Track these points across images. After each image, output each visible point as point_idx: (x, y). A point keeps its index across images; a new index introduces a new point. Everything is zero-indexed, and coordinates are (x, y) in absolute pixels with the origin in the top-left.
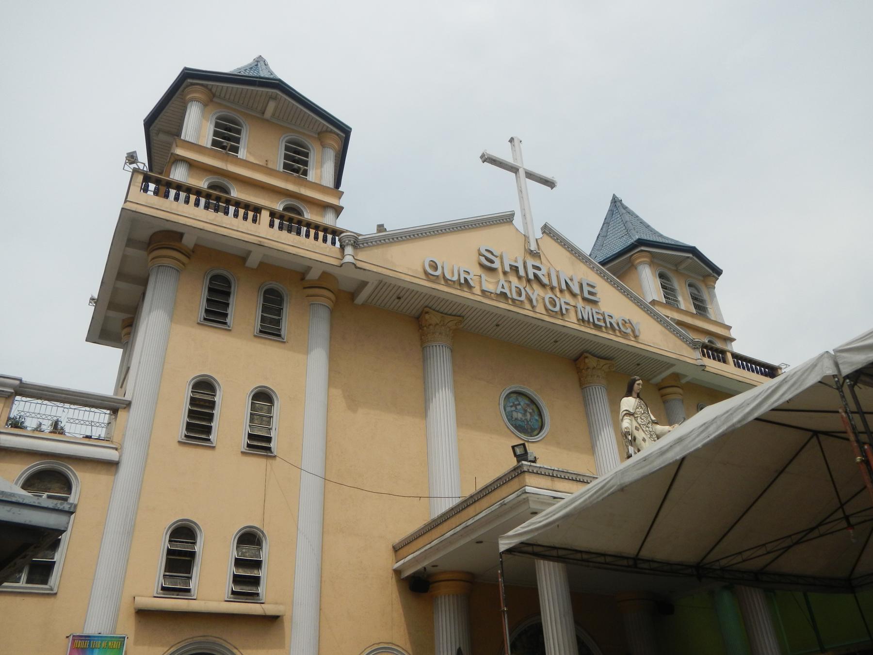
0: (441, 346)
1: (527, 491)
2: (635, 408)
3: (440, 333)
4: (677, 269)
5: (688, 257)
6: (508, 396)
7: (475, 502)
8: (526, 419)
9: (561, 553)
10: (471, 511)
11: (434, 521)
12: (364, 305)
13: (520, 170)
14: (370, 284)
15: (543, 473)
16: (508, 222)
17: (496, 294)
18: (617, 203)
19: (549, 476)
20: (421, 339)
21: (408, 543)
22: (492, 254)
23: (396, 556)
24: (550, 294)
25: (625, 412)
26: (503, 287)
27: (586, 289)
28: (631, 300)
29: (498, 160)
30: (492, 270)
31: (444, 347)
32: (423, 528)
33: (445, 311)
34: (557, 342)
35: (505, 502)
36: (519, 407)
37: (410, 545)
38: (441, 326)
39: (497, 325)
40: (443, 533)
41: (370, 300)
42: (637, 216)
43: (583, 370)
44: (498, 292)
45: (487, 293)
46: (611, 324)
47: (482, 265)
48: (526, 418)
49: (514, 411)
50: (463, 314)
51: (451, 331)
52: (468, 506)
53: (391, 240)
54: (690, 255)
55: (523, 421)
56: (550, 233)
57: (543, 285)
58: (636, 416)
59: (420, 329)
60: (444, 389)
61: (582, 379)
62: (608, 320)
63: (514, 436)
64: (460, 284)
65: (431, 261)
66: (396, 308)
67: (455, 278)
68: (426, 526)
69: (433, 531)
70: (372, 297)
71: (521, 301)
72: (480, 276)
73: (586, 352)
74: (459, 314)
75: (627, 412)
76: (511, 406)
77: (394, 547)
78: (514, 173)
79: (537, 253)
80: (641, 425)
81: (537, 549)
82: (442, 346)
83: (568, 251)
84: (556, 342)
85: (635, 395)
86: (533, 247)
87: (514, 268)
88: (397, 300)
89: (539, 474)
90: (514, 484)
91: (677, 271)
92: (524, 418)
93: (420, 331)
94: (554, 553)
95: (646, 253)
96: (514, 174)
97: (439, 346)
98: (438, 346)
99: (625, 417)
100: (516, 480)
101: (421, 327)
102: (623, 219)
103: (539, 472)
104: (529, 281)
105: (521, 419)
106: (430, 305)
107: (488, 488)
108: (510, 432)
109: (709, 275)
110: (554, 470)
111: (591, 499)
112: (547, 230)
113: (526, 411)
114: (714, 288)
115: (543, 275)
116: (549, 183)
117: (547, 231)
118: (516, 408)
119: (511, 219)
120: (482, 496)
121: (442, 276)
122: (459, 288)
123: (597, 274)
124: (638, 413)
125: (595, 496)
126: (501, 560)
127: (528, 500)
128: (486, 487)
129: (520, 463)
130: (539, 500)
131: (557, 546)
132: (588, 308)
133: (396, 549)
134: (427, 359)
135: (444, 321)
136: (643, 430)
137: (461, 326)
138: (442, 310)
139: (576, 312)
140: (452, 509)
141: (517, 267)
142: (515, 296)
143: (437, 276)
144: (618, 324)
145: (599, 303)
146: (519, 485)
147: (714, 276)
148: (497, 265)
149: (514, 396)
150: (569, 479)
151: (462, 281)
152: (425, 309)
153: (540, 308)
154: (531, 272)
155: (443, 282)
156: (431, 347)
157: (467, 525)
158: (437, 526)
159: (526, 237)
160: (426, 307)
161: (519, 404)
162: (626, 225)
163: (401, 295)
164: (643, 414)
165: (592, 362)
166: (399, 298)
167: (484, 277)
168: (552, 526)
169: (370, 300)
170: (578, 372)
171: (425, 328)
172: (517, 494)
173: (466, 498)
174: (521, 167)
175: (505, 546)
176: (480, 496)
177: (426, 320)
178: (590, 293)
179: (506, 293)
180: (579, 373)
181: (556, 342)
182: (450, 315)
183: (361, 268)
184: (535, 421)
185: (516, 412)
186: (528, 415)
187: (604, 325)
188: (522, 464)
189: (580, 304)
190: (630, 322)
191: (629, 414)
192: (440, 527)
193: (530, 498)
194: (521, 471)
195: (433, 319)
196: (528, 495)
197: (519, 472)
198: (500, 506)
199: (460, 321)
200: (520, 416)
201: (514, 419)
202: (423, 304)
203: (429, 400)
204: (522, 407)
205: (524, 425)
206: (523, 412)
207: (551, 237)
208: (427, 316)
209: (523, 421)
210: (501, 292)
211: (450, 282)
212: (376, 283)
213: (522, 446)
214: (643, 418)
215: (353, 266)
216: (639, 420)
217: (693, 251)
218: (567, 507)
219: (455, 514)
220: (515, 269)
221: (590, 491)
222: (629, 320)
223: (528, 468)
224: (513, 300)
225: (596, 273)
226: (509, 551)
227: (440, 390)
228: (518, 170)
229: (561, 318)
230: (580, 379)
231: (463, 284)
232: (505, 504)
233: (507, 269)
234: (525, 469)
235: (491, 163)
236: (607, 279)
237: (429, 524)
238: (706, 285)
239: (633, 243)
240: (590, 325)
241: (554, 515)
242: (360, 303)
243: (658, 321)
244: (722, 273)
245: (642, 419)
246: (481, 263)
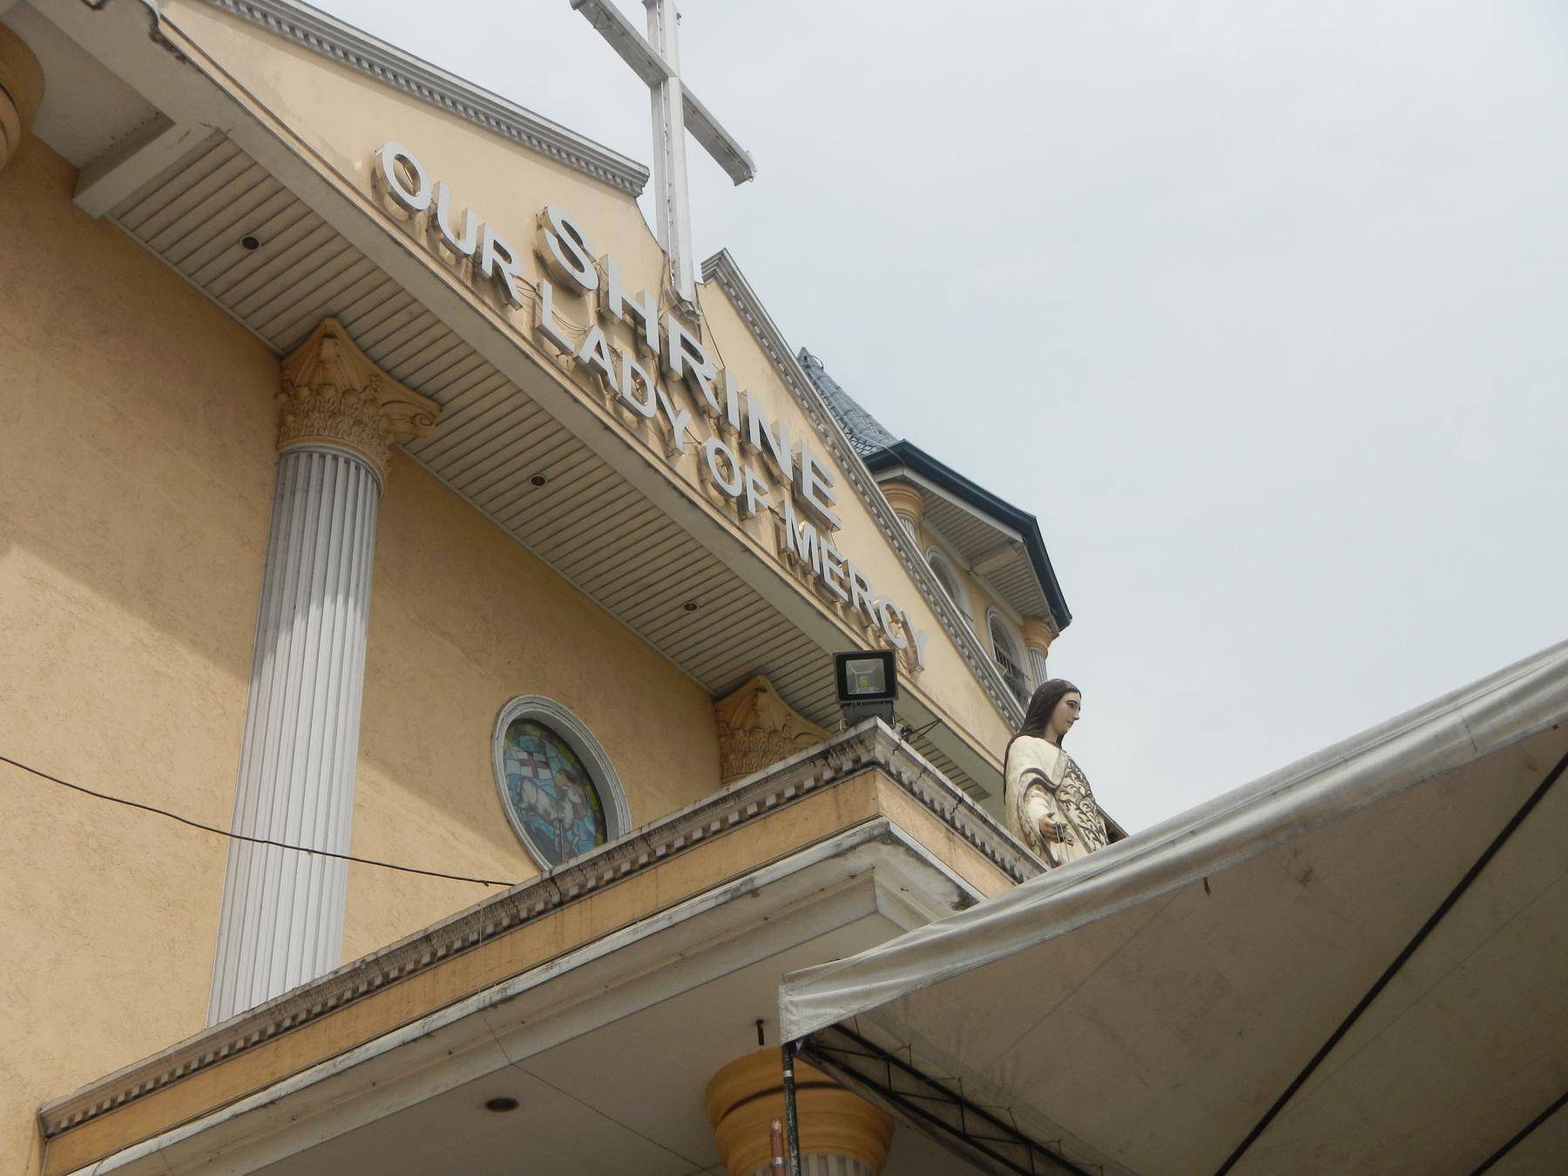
0: (353, 466)
1: (896, 830)
2: (1060, 772)
3: (358, 422)
4: (972, 568)
5: (1012, 542)
6: (519, 726)
7: (561, 904)
8: (561, 821)
9: (973, 1125)
10: (534, 940)
11: (306, 993)
12: (104, 226)
13: (673, 83)
14: (169, 136)
15: (927, 799)
16: (623, 191)
17: (577, 359)
18: (814, 369)
19: (943, 817)
20: (281, 424)
21: (129, 1100)
22: (579, 241)
23: (42, 1156)
24: (713, 442)
25: (1033, 776)
26: (598, 348)
27: (809, 478)
28: (906, 569)
29: (618, 18)
30: (569, 289)
31: (363, 472)
32: (234, 1029)
33: (389, 362)
34: (695, 607)
35: (757, 883)
36: (544, 774)
37: (139, 1105)
38: (365, 402)
39: (538, 481)
40: (345, 1044)
41: (132, 220)
42: (868, 416)
43: (741, 733)
44: (587, 360)
45: (546, 340)
46: (863, 604)
47: (540, 259)
48: (561, 815)
49: (529, 779)
50: (445, 395)
51: (390, 440)
52: (517, 923)
53: (286, 28)
54: (1019, 538)
55: (551, 823)
56: (729, 285)
57: (700, 411)
58: (1064, 797)
59: (284, 390)
60: (340, 599)
61: (732, 757)
62: (856, 588)
63: (526, 858)
64: (476, 273)
65: (401, 158)
66: (218, 286)
67: (467, 247)
68: (255, 1017)
69: (286, 1042)
70: (140, 213)
71: (640, 417)
72: (536, 290)
73: (767, 674)
74: (430, 387)
75: (1038, 776)
76: (523, 763)
77: (42, 1119)
78: (649, 85)
79: (694, 313)
80: (1082, 830)
81: (903, 1083)
82: (358, 468)
83: (768, 358)
84: (690, 607)
85: (1050, 730)
86: (686, 293)
87: (628, 319)
88: (238, 251)
89: (914, 794)
90: (818, 812)
91: (968, 575)
92: (554, 815)
93: (283, 397)
94: (950, 1115)
95: (910, 489)
96: (648, 90)
97: (347, 462)
98: (341, 461)
99: (1034, 791)
100: (825, 799)
101: (286, 386)
102: (834, 403)
103: (916, 789)
104: (664, 375)
105: (546, 811)
106: (348, 315)
107: (654, 840)
108: (512, 840)
109: (1038, 618)
110: (961, 800)
111: (1484, 727)
112: (720, 270)
113: (562, 795)
114: (1046, 655)
115: (708, 379)
116: (735, 164)
117: (720, 274)
118: (536, 775)
119: (638, 190)
120: (608, 875)
121: (422, 221)
122: (469, 285)
123: (832, 455)
124: (1069, 789)
125: (1512, 712)
126: (788, 1073)
127: (871, 881)
128: (645, 838)
129: (866, 726)
130: (903, 895)
131: (970, 1091)
132: (805, 530)
133: (50, 1129)
134: (293, 492)
135: (376, 391)
136: (1086, 845)
137: (431, 433)
138: (379, 351)
139: (778, 532)
140: (427, 938)
141: (638, 320)
142: (628, 395)
143: (411, 211)
144: (878, 613)
145: (835, 534)
146: (839, 818)
147: (1048, 624)
148: (588, 279)
149: (534, 734)
150: (992, 857)
151: (487, 268)
152: (328, 322)
153: (685, 466)
154: (677, 355)
155: (424, 242)
156: (316, 457)
157: (510, 992)
158: (313, 1017)
159: (669, 264)
160: (334, 316)
161: (546, 765)
162: (845, 418)
163: (260, 235)
164: (1084, 797)
165: (771, 711)
166: (251, 243)
167: (547, 289)
168: (1181, 882)
169: (140, 213)
170: (719, 737)
171: (305, 392)
172: (839, 845)
173: (514, 891)
174: (674, 76)
175: (811, 1012)
176: (600, 878)
177: (321, 362)
178: (817, 491)
179: (604, 373)
180: (723, 739)
181: (690, 607)
182: (401, 381)
183: (170, 47)
184: (584, 837)
185: (535, 784)
186: (568, 814)
187: (845, 596)
188: (876, 727)
189: (790, 513)
190: (905, 625)
191: (1041, 782)
192: (339, 1018)
193: (879, 877)
194: (857, 761)
195: (345, 369)
196: (885, 851)
197: (847, 766)
198: (729, 896)
199: (434, 416)
200: (544, 802)
201: (523, 805)
202: (325, 303)
203: (278, 627)
204: (553, 778)
205: (552, 837)
206: (555, 795)
207: (730, 299)
208: (329, 349)
209: (551, 823)
210: (592, 359)
211: (446, 254)
212: (199, 135)
213: (881, 661)
214: (1084, 809)
215: (145, 25)
216: (1073, 814)
217: (1027, 526)
218: (1289, 788)
219: (436, 961)
220: (635, 325)
221: (1461, 701)
222: (902, 613)
223: (889, 754)
224: (620, 401)
225: (829, 452)
226: (813, 1048)
227: (328, 600)
228: (665, 78)
229: (737, 523)
230: (723, 759)
231: (484, 279)
232: (754, 893)
233: (616, 307)
234: (880, 752)
235: (595, 23)
236: (856, 482)
237: (274, 1010)
238: (1028, 642)
239: (885, 451)
240: (806, 581)
241: (1193, 833)
242: (96, 215)
243: (961, 655)
244: (1067, 624)
245: (1082, 813)
246: (546, 256)
